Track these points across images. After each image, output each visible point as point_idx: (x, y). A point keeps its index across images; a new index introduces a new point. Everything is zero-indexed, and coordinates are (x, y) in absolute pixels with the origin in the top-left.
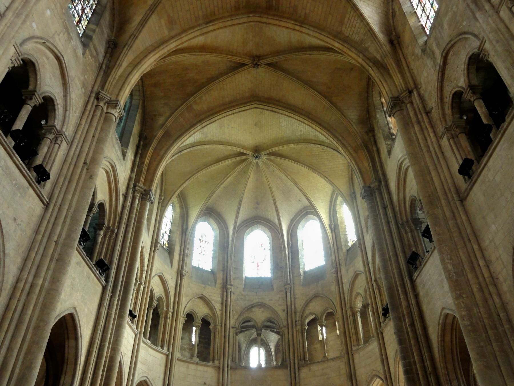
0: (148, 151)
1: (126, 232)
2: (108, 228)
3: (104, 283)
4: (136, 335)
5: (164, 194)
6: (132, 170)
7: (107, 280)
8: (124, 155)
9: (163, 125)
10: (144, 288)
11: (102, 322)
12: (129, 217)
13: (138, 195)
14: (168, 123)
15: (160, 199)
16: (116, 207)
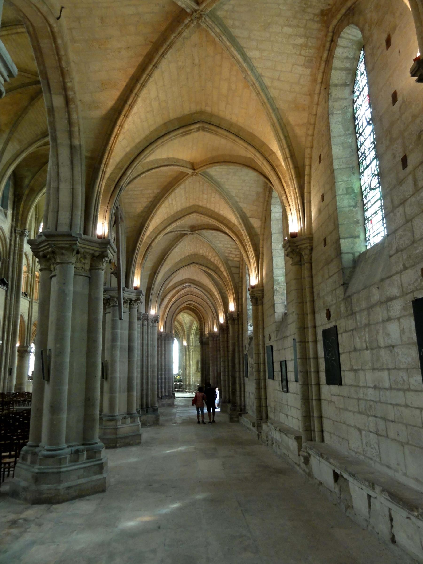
0: (20, 204)
1: (14, 259)
2: (4, 259)
3: (5, 288)
4: (30, 302)
5: (39, 213)
6: (12, 220)
7: (7, 287)
8: (6, 215)
9: (28, 185)
10: (31, 276)
11: (8, 307)
12: (15, 250)
13: (18, 235)
14: (31, 184)
15: (36, 218)
16: (6, 249)
